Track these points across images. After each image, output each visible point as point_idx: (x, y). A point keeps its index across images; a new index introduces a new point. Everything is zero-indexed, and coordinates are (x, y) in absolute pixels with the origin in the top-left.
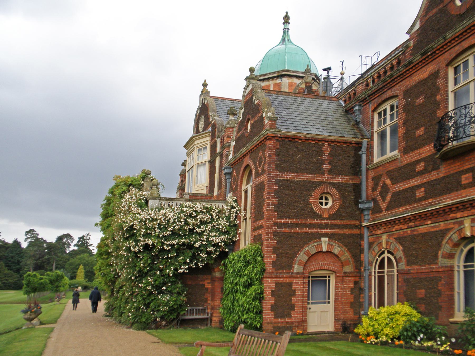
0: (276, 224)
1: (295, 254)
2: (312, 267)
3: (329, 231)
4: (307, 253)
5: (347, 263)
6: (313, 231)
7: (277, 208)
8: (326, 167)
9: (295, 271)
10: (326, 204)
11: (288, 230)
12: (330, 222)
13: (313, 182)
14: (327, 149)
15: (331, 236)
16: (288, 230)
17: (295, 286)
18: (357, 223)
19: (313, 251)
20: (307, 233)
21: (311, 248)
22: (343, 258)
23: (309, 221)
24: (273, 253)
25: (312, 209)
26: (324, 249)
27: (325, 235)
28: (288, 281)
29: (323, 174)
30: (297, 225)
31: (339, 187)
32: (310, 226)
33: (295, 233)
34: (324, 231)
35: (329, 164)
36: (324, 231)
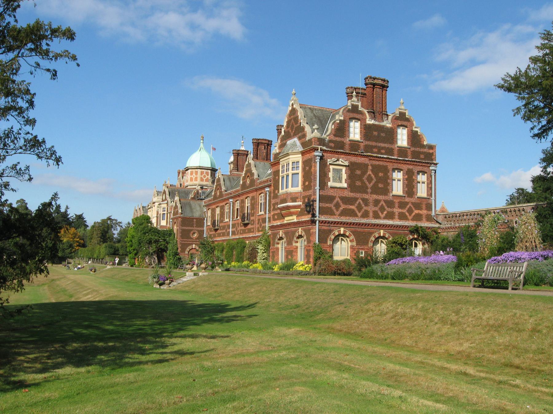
1: (186, 249)
7: (181, 236)
14: (195, 220)
15: (195, 244)
21: (190, 247)
31: (198, 231)
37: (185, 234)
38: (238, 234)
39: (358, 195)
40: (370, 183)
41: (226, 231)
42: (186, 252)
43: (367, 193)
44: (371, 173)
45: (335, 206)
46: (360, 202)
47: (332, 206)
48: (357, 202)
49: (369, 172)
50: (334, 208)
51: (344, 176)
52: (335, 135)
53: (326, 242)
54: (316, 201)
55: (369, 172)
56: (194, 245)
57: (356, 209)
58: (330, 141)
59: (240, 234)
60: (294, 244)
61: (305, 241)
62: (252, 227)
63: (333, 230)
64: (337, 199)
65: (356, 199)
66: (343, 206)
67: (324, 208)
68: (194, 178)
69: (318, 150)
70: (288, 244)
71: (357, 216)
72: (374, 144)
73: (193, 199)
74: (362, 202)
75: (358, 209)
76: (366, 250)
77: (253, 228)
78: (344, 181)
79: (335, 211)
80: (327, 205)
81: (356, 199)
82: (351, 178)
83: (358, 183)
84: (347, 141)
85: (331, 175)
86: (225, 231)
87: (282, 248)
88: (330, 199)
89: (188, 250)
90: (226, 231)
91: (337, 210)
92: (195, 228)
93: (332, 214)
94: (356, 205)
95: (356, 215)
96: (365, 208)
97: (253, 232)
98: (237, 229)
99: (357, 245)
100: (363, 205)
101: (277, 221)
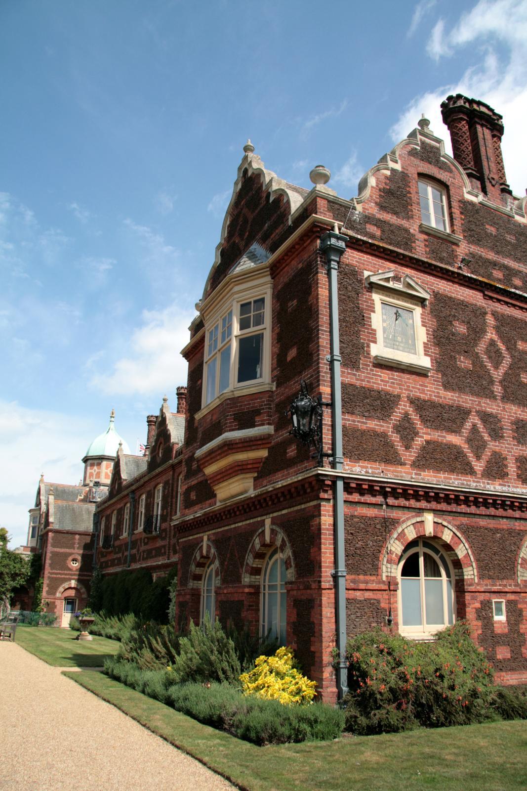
0: (49, 573)
4: (64, 587)
5: (84, 593)
6: (68, 577)
11: (55, 576)
16: (55, 576)
17: (56, 603)
18: (90, 574)
19: (67, 587)
20: (64, 578)
21: (66, 585)
22: (82, 591)
23: (66, 572)
25: (67, 566)
27: (73, 579)
28: (53, 600)
29: (74, 549)
30: (60, 574)
32: (66, 574)
35: (78, 543)
39: (467, 401)
40: (496, 367)
41: (123, 554)
43: (492, 396)
44: (495, 337)
45: (398, 429)
46: (474, 425)
47: (386, 427)
48: (468, 425)
49: (491, 334)
50: (395, 438)
51: (422, 335)
52: (382, 207)
53: (375, 569)
54: (332, 405)
55: (491, 334)
57: (466, 448)
58: (368, 219)
59: (144, 559)
60: (246, 579)
61: (287, 564)
63: (395, 522)
64: (404, 407)
65: (464, 413)
66: (425, 435)
67: (363, 433)
68: (95, 474)
69: (333, 228)
70: (224, 581)
71: (471, 471)
72: (491, 256)
73: (81, 501)
74: (480, 426)
75: (471, 447)
76: (511, 597)
77: (164, 546)
78: (420, 348)
79: (400, 447)
80: (373, 424)
81: (464, 413)
82: (442, 340)
83: (464, 363)
84: (414, 229)
85: (379, 319)
86: (120, 555)
87: (209, 591)
88: (382, 404)
90: (123, 554)
91: (408, 447)
93: (391, 458)
94: (465, 432)
95: (469, 470)
96: (493, 446)
98: (138, 551)
99: (481, 577)
100: (486, 437)
101: (196, 508)
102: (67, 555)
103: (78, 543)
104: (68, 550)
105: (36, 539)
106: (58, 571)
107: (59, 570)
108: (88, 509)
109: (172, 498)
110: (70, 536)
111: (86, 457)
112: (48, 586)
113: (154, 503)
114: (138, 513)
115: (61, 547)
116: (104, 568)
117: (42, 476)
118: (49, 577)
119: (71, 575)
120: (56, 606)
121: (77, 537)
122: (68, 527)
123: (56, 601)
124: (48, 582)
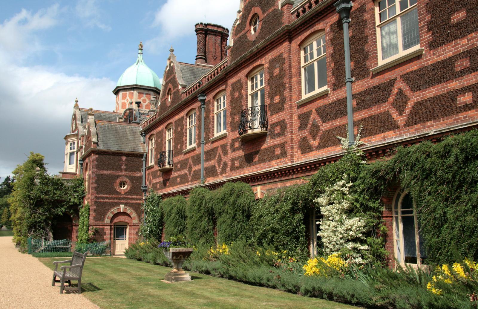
0: (96, 197)
1: (106, 213)
2: (116, 220)
3: (124, 201)
5: (134, 218)
6: (116, 201)
7: (96, 189)
8: (124, 167)
9: (106, 222)
10: (124, 187)
11: (102, 201)
12: (125, 196)
13: (116, 175)
15: (125, 204)
16: (102, 201)
17: (105, 230)
20: (112, 202)
22: (132, 216)
23: (114, 196)
24: (94, 212)
26: (122, 210)
29: (121, 171)
30: (107, 198)
31: (131, 178)
32: (114, 198)
33: (106, 202)
34: (122, 201)
35: (126, 165)
36: (122, 201)
37: (103, 184)
38: (224, 171)
41: (190, 168)
42: (107, 221)
56: (122, 206)
59: (233, 169)
62: (277, 141)
77: (282, 146)
86: (186, 171)
89: (110, 215)
92: (124, 173)
97: (284, 154)
102: (114, 178)
103: (126, 165)
104: (114, 173)
105: (75, 165)
106: (106, 196)
107: (107, 194)
108: (132, 130)
109: (290, 77)
110: (116, 158)
111: (117, 87)
112: (95, 211)
113: (247, 95)
114: (213, 117)
115: (107, 170)
116: (159, 189)
117: (77, 102)
118: (96, 202)
119: (120, 199)
120: (105, 233)
121: (124, 158)
122: (113, 147)
123: (106, 227)
124: (95, 207)
